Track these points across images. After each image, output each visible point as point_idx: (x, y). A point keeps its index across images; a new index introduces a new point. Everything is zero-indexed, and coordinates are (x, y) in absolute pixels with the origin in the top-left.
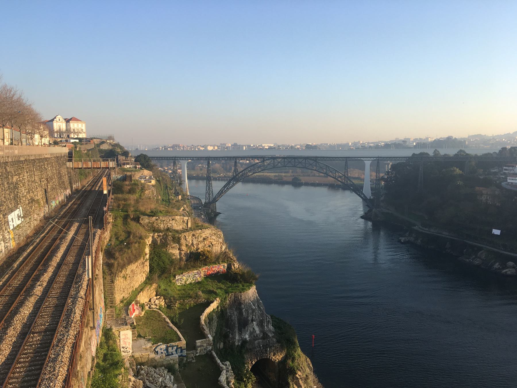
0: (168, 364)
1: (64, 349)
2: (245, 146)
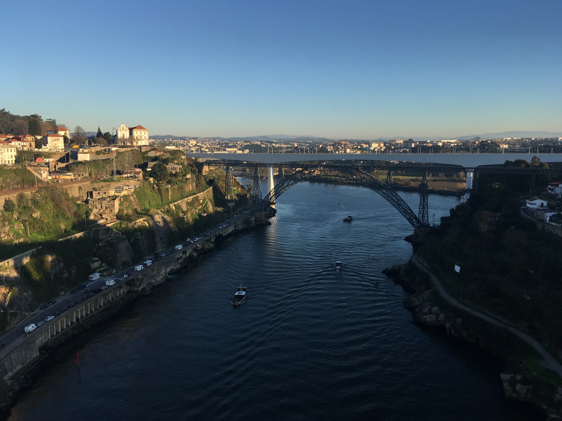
2: (415, 142)
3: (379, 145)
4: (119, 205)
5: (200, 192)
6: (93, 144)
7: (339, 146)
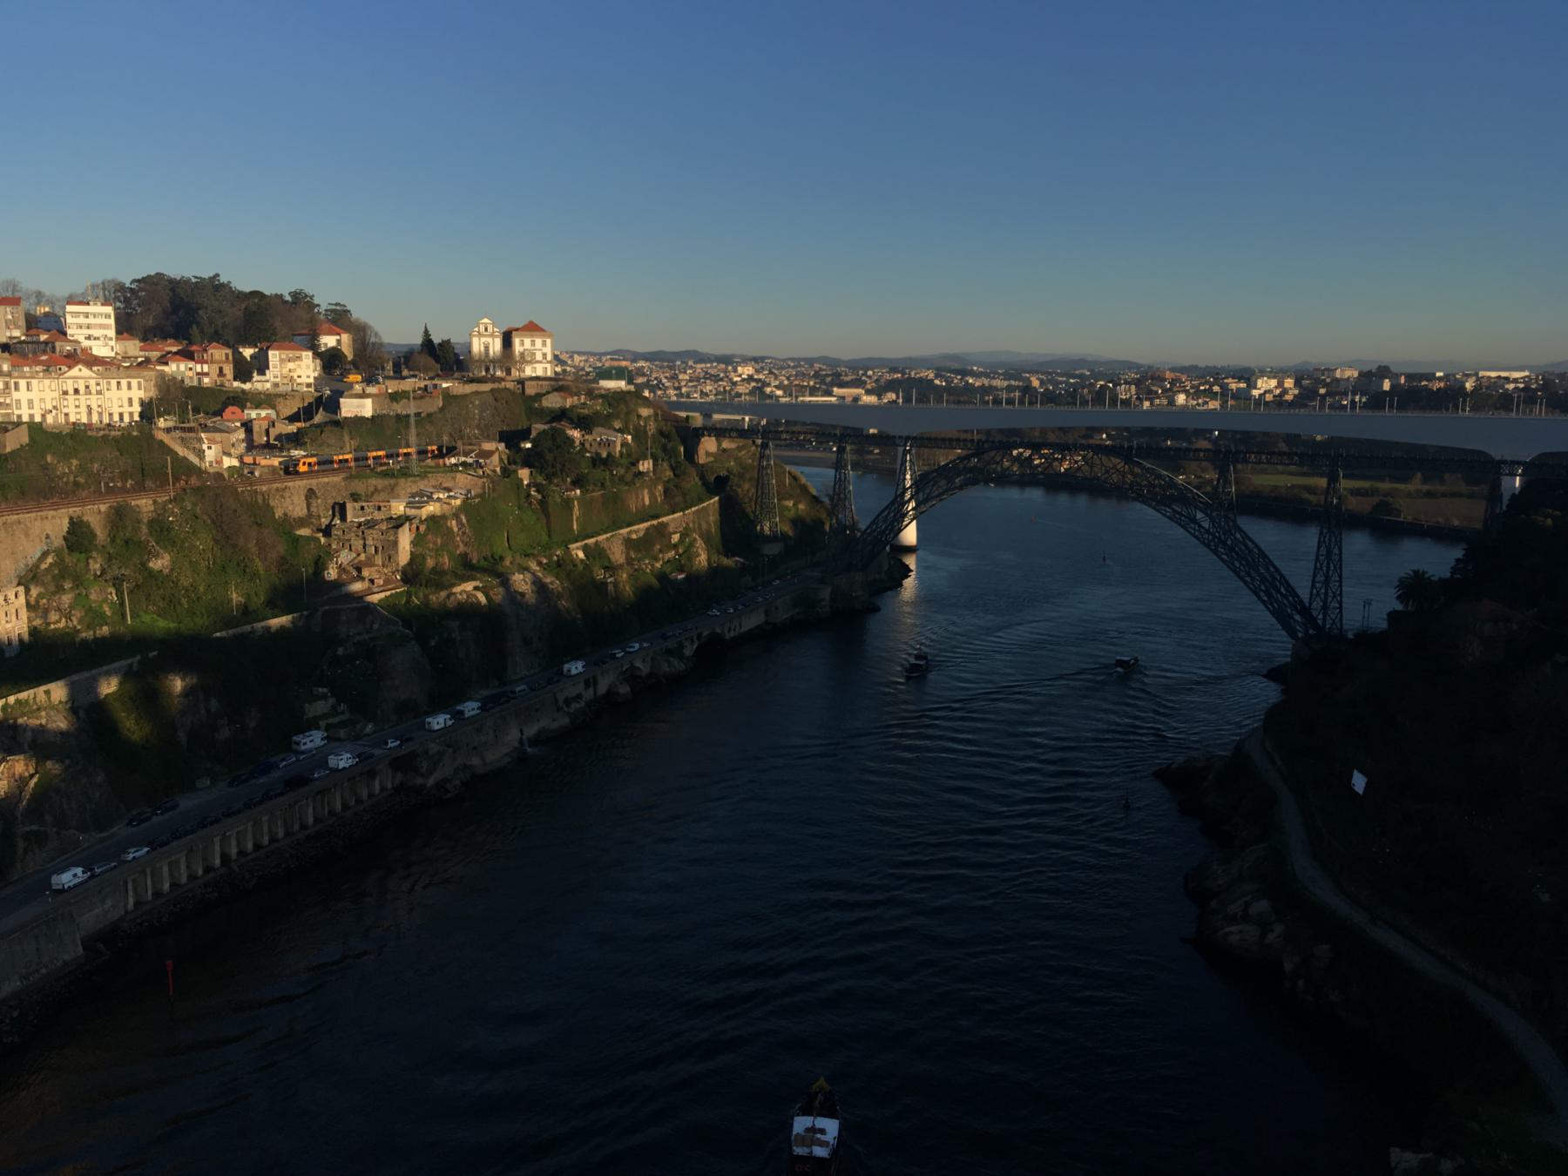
2: (1394, 377)
3: (1280, 384)
4: (412, 542)
5: (674, 513)
6: (405, 372)
7: (1154, 386)
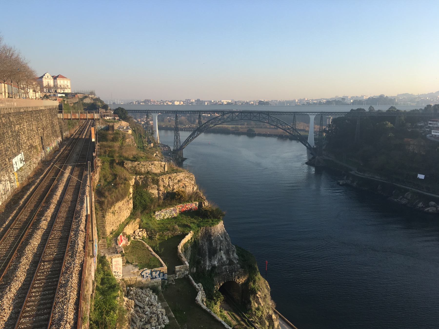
0: (153, 286)
1: (73, 276)
2: (207, 102)
